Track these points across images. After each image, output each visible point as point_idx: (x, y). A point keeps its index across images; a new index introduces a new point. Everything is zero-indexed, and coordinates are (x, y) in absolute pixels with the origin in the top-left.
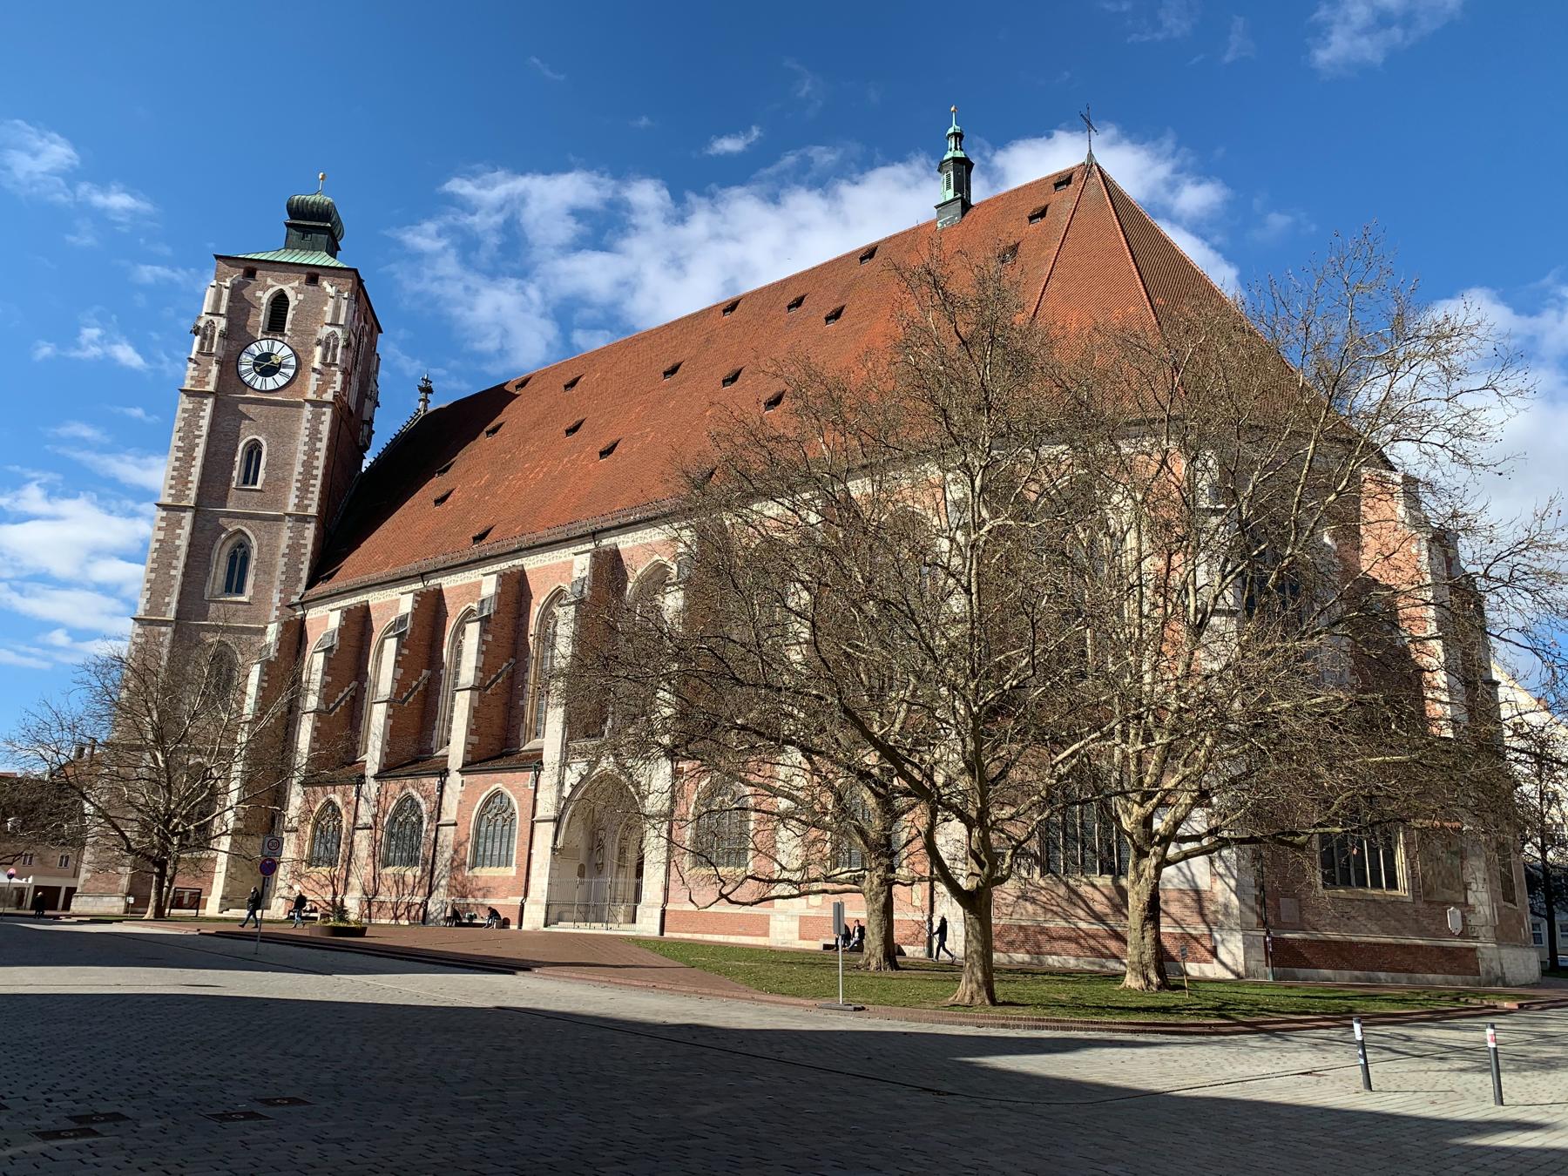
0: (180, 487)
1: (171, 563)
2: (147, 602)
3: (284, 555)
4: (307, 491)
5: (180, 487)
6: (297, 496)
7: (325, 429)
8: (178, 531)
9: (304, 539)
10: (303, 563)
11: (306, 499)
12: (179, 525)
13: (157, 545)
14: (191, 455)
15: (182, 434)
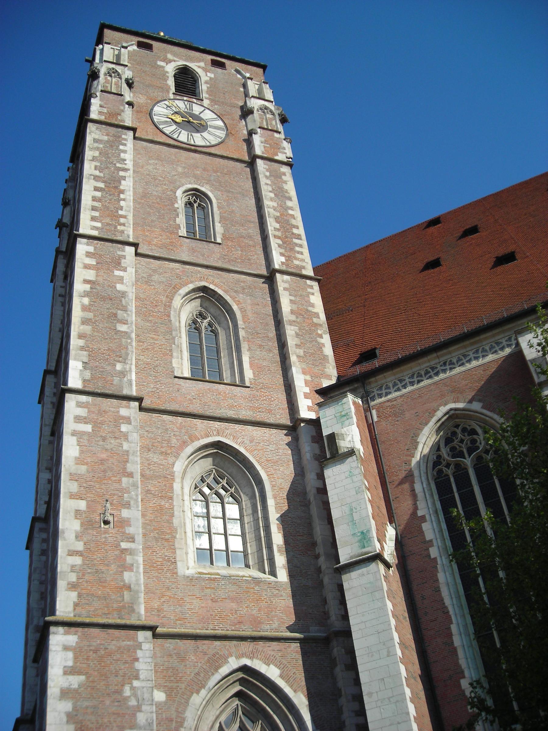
0: (108, 220)
1: (115, 315)
2: (85, 368)
3: (291, 323)
4: (292, 249)
5: (108, 220)
6: (282, 254)
7: (290, 187)
8: (117, 273)
9: (313, 306)
10: (321, 336)
11: (296, 259)
12: (117, 263)
13: (87, 287)
14: (116, 187)
15: (98, 164)
